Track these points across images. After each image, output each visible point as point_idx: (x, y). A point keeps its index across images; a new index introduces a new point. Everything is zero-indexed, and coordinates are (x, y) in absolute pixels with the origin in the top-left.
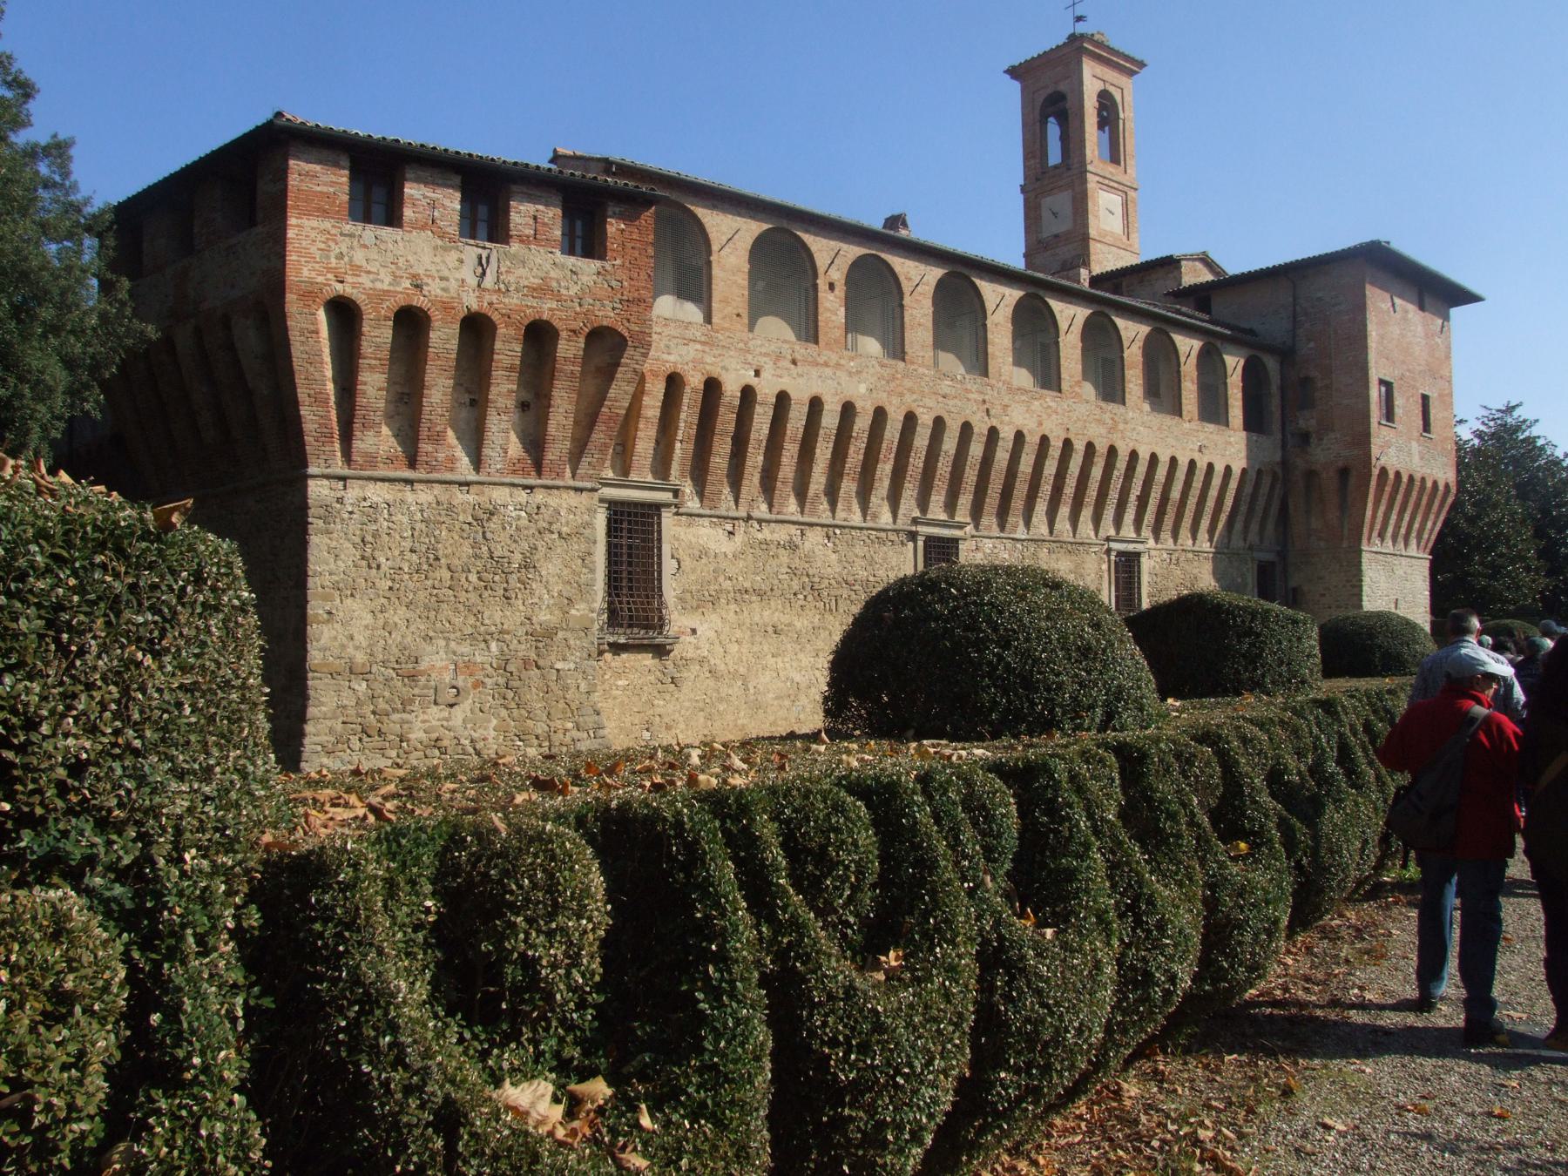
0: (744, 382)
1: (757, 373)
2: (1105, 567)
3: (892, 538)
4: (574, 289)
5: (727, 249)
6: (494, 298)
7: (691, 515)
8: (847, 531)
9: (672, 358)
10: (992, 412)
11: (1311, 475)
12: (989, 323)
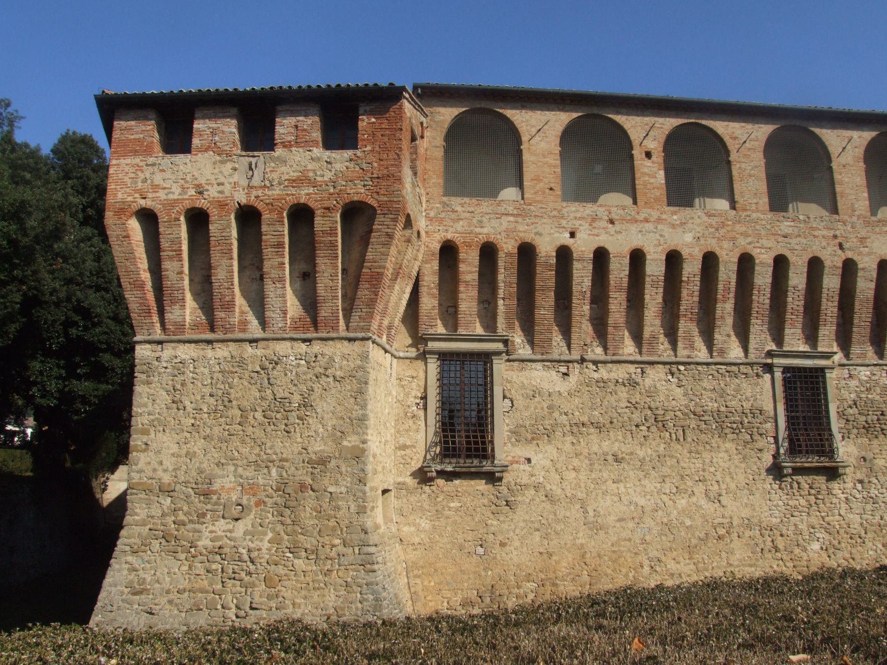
0: (558, 243)
1: (572, 235)
3: (745, 371)
4: (328, 176)
5: (537, 138)
6: (260, 193)
7: (523, 361)
8: (692, 366)
9: (485, 231)
10: (846, 245)
12: (834, 165)
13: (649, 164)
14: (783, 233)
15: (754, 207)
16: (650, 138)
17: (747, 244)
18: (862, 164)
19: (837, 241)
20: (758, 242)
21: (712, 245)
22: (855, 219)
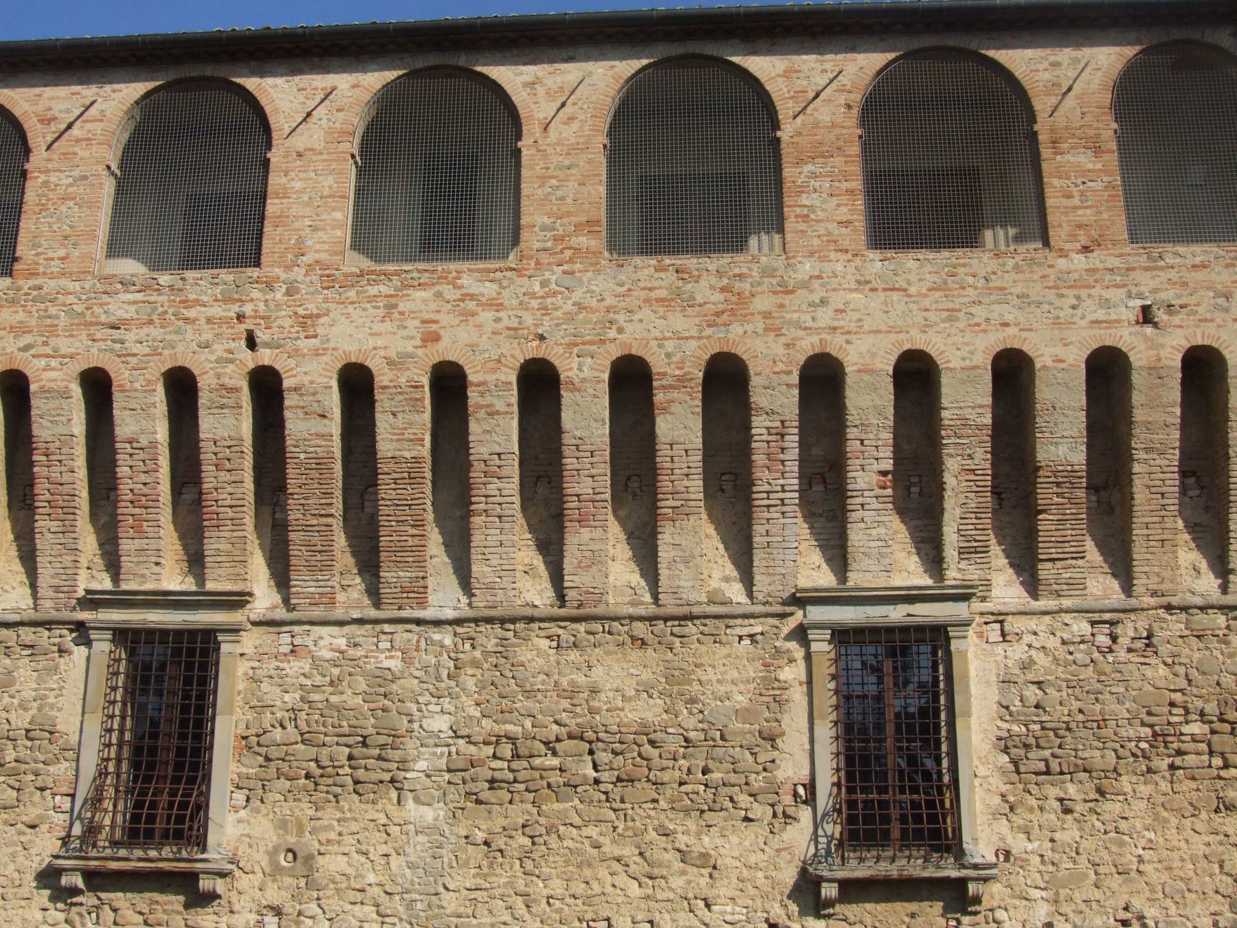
2: (793, 673)
10: (261, 336)
14: (112, 319)
15: (55, 267)
17: (20, 350)
19: (243, 327)
20: (45, 344)
22: (298, 273)
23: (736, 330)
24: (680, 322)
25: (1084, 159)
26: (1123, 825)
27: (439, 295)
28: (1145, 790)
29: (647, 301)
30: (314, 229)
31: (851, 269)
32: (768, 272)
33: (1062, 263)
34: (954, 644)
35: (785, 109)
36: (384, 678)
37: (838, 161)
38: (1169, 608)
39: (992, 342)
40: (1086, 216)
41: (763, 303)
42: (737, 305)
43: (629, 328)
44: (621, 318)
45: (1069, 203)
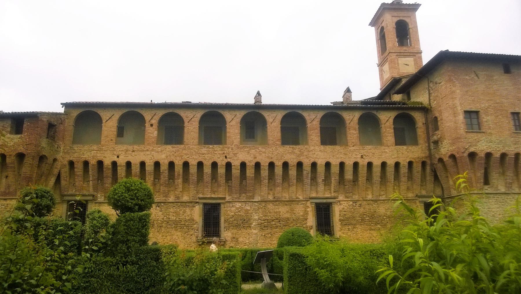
0: (112, 160)
1: (118, 157)
3: (188, 205)
7: (100, 203)
8: (167, 203)
9: (84, 156)
10: (228, 157)
11: (441, 160)
12: (227, 126)
13: (151, 129)
14: (203, 153)
16: (153, 119)
17: (187, 158)
18: (239, 125)
19: (225, 155)
20: (191, 157)
21: (172, 159)
23: (301, 158)
24: (293, 156)
25: (354, 132)
26: (357, 232)
27: (256, 151)
28: (360, 227)
29: (288, 153)
30: (235, 139)
31: (318, 148)
32: (306, 148)
33: (350, 148)
34: (333, 205)
35: (308, 121)
36: (247, 210)
37: (316, 131)
38: (364, 200)
39: (340, 160)
40: (354, 141)
41: (305, 154)
42: (302, 154)
43: (286, 157)
44: (284, 155)
45: (351, 138)
